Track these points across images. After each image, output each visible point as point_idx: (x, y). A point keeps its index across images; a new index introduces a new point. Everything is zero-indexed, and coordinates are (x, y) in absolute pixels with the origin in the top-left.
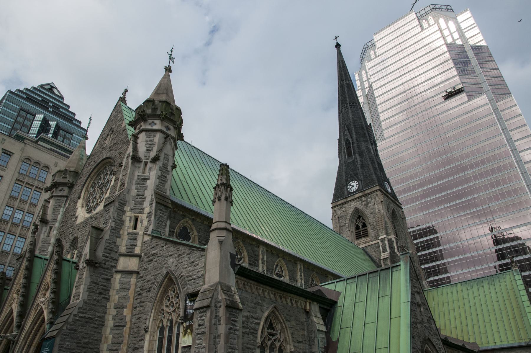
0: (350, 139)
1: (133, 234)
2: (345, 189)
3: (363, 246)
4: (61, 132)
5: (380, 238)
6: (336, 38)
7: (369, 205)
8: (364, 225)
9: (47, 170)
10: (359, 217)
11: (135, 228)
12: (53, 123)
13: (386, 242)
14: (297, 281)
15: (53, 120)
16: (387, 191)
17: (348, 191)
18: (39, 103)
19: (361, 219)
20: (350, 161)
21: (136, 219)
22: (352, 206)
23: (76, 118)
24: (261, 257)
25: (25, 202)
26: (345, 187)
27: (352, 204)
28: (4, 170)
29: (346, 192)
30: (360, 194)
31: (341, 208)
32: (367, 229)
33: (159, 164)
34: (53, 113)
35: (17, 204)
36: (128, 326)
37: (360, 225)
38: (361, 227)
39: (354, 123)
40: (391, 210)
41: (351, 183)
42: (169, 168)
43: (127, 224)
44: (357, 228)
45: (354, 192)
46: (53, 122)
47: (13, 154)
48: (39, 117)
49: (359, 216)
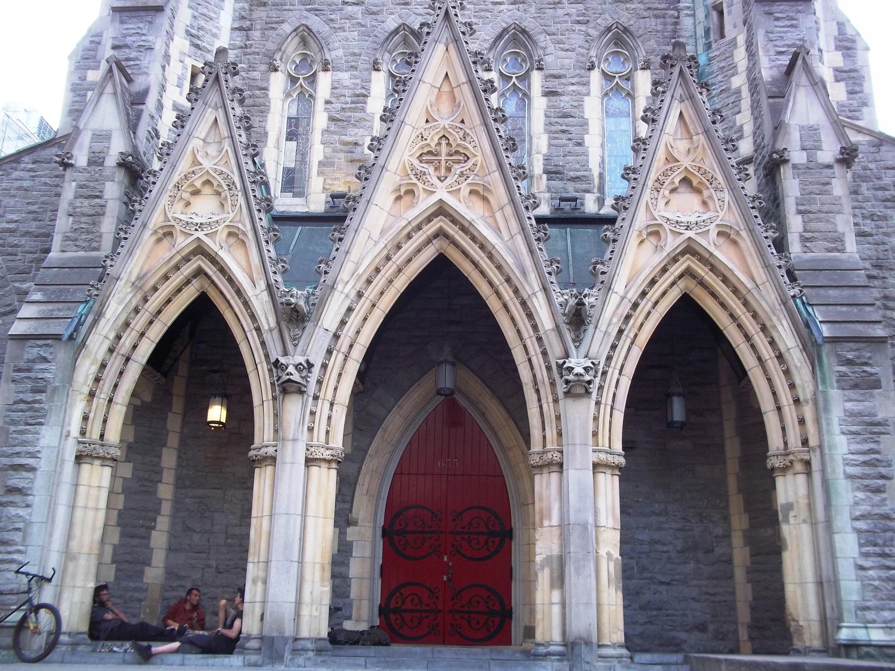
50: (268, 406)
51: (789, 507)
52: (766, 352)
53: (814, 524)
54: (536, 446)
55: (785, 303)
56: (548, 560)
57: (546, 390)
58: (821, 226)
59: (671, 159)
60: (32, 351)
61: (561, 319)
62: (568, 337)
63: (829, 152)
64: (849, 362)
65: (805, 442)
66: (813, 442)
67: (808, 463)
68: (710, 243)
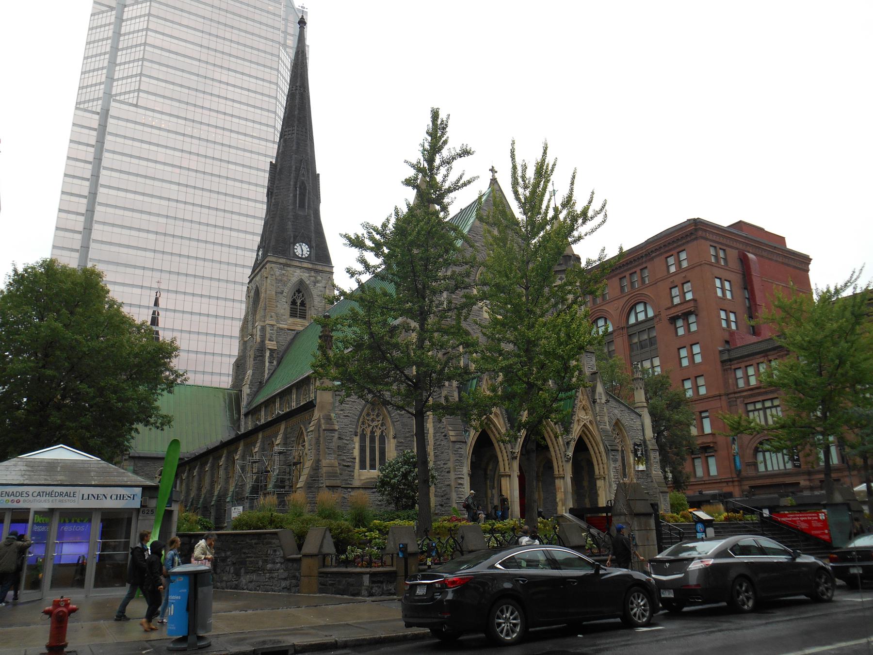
7: (318, 285)
10: (299, 291)
17: (294, 253)
19: (301, 295)
22: (296, 274)
26: (292, 245)
27: (297, 271)
29: (292, 252)
30: (310, 266)
31: (281, 269)
32: (305, 310)
37: (299, 302)
38: (298, 304)
41: (304, 244)
44: (294, 303)
49: (299, 289)
50: (506, 462)
51: (600, 487)
52: (597, 452)
53: (605, 491)
54: (556, 472)
55: (602, 440)
56: (561, 500)
57: (560, 459)
58: (603, 419)
59: (581, 402)
60: (458, 446)
61: (565, 443)
62: (566, 447)
63: (603, 401)
64: (613, 455)
65: (604, 473)
66: (606, 473)
67: (604, 478)
68: (588, 424)
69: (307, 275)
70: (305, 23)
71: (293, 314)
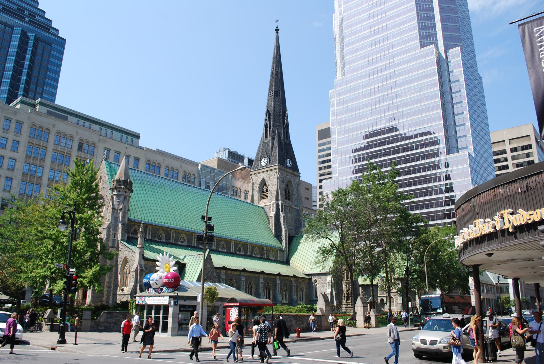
0: (268, 124)
1: (114, 239)
2: (259, 163)
3: (264, 205)
4: (40, 43)
5: (272, 202)
6: (277, 21)
7: (271, 178)
8: (267, 191)
9: (48, 132)
11: (115, 237)
12: (31, 35)
13: (275, 206)
14: (192, 243)
15: (32, 31)
16: (286, 167)
18: (15, 14)
20: (266, 141)
21: (115, 234)
23: (53, 26)
24: (172, 235)
25: (37, 158)
28: (19, 137)
30: (267, 169)
33: (123, 211)
34: (31, 22)
35: (31, 160)
36: (114, 271)
37: (265, 190)
39: (274, 110)
40: (285, 181)
42: (127, 211)
43: (111, 236)
45: (264, 166)
46: (32, 34)
47: (24, 122)
48: (18, 29)
69: (266, 174)
70: (278, 30)
71: (263, 198)
